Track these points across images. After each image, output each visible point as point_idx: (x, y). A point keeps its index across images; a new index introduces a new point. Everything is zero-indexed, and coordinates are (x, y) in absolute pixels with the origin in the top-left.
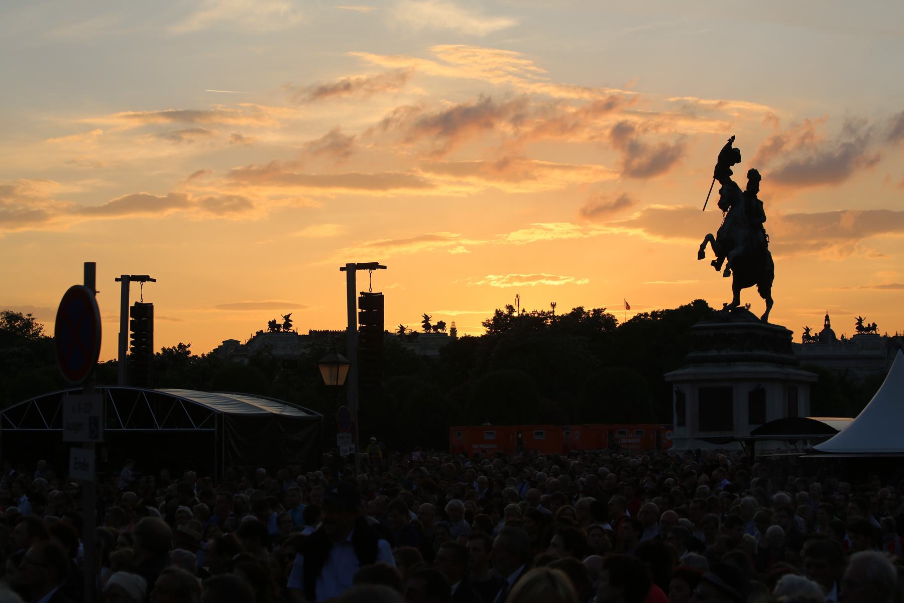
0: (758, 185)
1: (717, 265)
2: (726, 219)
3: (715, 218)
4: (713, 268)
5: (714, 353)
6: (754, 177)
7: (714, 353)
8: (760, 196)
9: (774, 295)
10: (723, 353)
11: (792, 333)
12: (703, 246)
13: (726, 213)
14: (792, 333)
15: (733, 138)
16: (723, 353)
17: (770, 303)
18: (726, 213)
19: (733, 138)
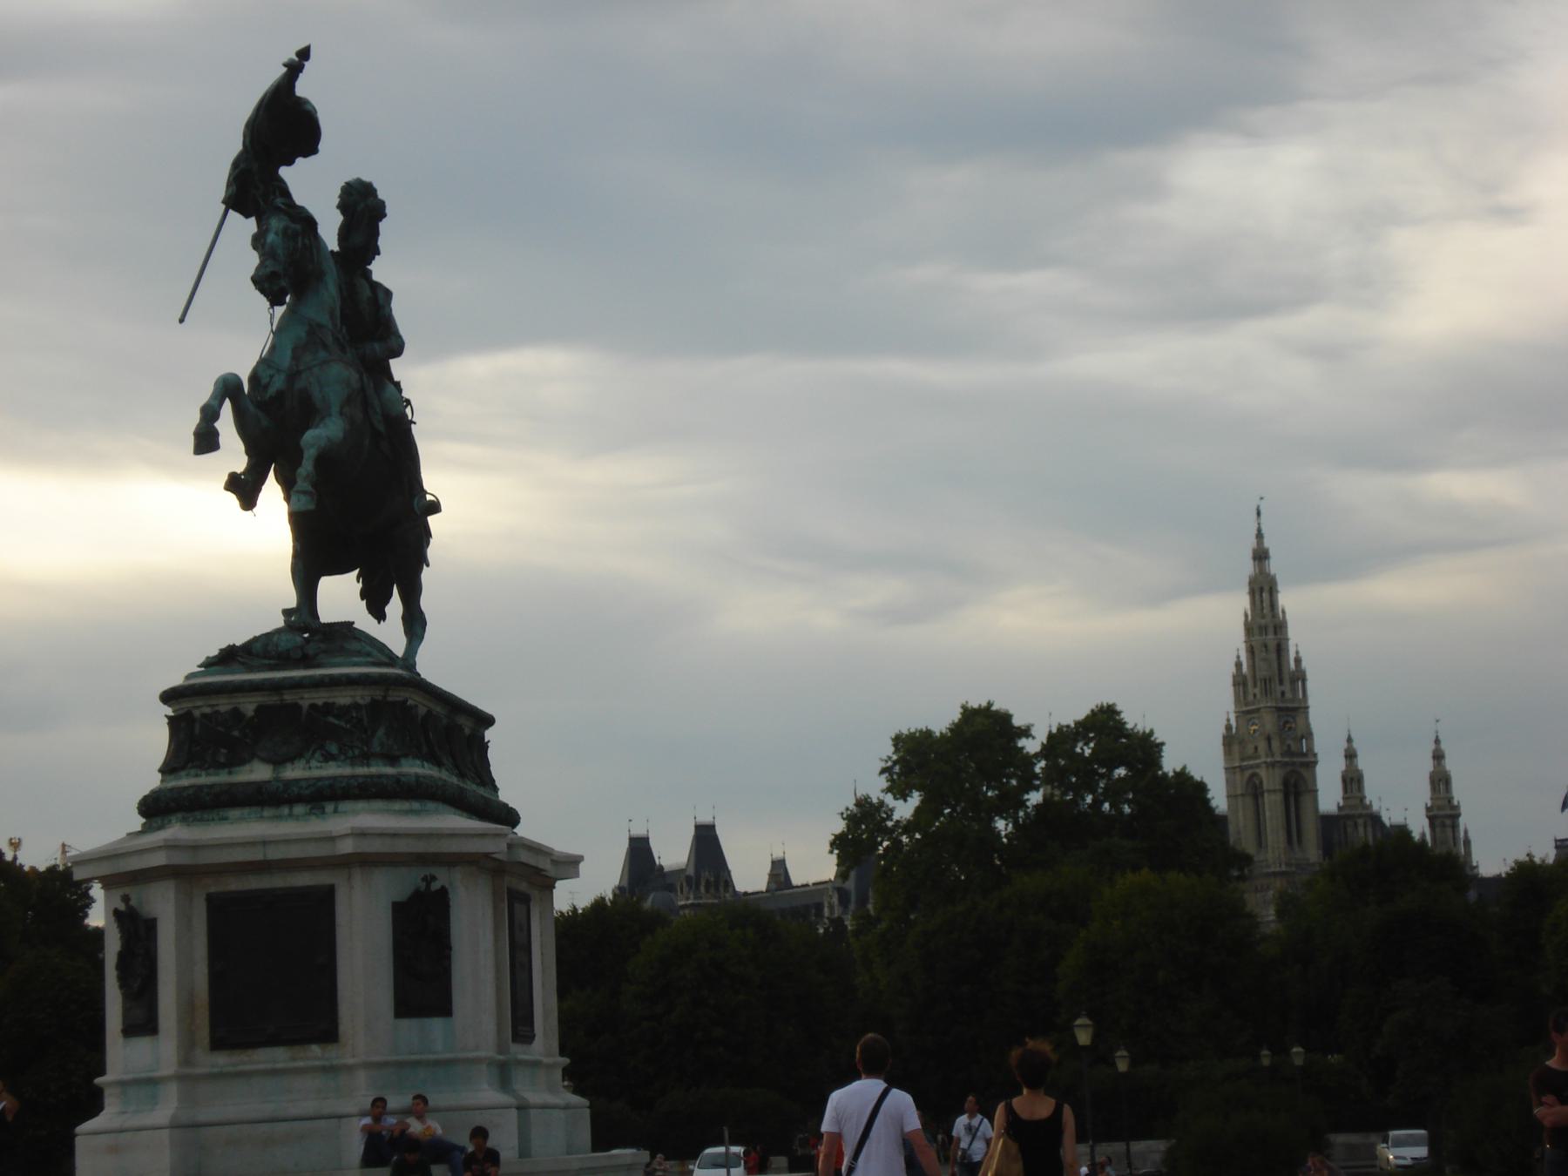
0: (375, 233)
1: (245, 489)
2: (278, 333)
3: (241, 332)
4: (232, 499)
5: (258, 772)
6: (362, 207)
7: (258, 772)
8: (380, 270)
9: (426, 602)
10: (293, 772)
11: (488, 721)
12: (210, 414)
13: (280, 311)
14: (488, 721)
15: (304, 54)
16: (293, 772)
17: (415, 623)
18: (280, 311)
19: (304, 54)
